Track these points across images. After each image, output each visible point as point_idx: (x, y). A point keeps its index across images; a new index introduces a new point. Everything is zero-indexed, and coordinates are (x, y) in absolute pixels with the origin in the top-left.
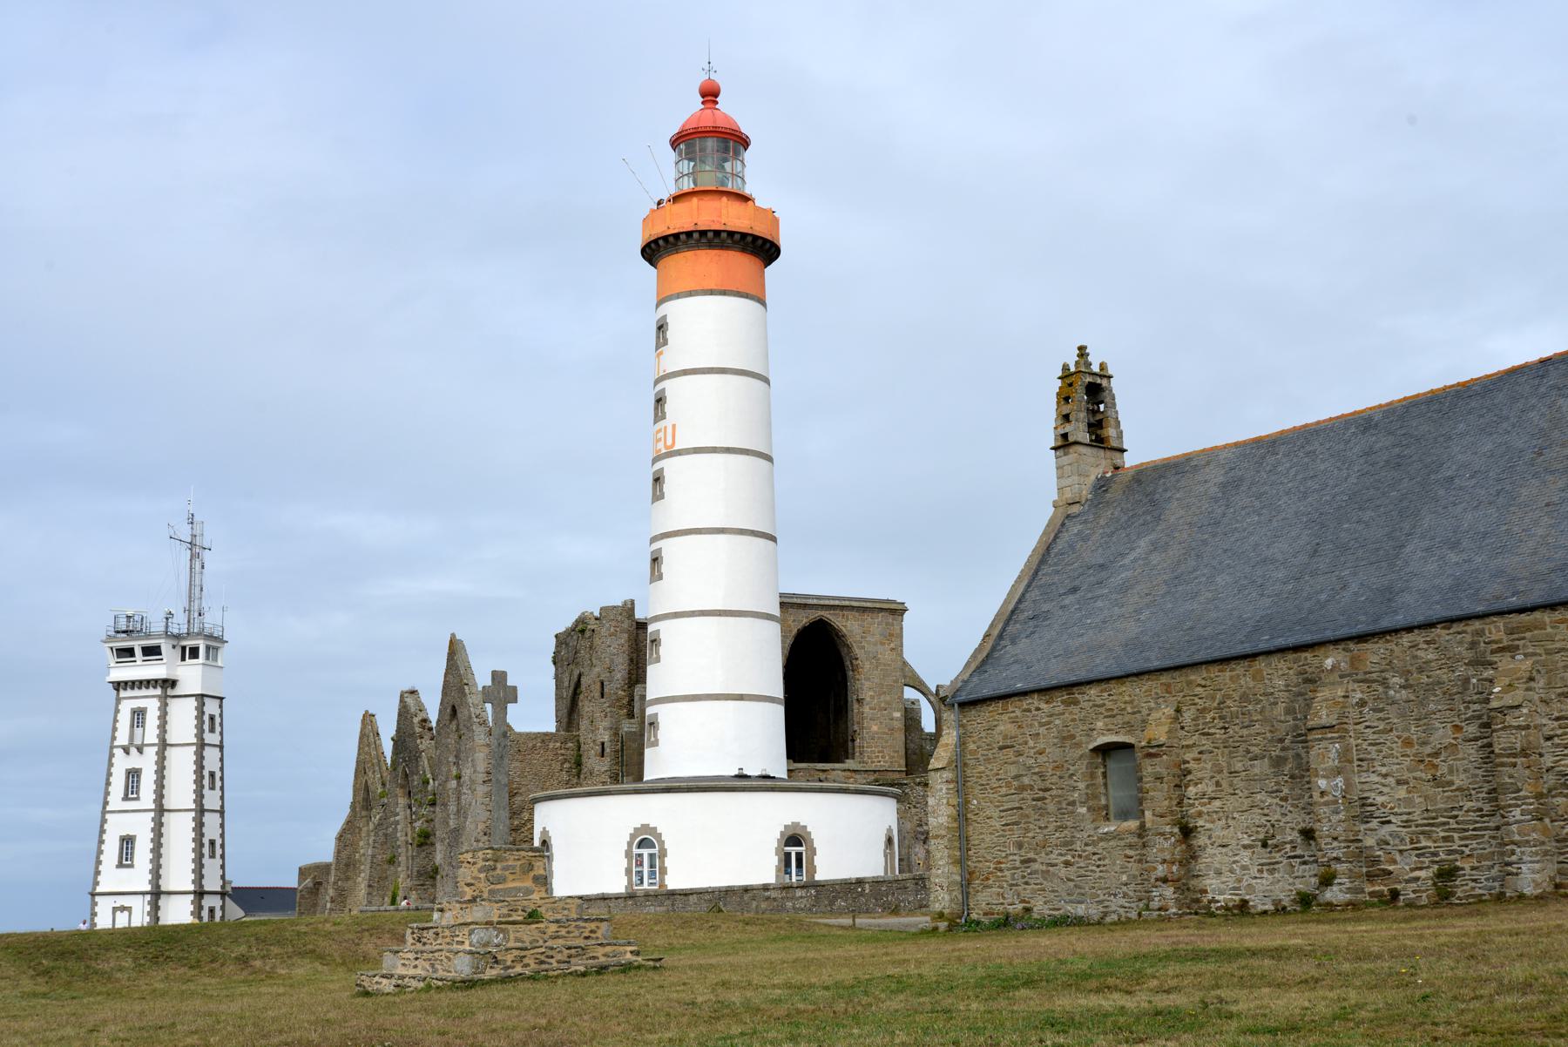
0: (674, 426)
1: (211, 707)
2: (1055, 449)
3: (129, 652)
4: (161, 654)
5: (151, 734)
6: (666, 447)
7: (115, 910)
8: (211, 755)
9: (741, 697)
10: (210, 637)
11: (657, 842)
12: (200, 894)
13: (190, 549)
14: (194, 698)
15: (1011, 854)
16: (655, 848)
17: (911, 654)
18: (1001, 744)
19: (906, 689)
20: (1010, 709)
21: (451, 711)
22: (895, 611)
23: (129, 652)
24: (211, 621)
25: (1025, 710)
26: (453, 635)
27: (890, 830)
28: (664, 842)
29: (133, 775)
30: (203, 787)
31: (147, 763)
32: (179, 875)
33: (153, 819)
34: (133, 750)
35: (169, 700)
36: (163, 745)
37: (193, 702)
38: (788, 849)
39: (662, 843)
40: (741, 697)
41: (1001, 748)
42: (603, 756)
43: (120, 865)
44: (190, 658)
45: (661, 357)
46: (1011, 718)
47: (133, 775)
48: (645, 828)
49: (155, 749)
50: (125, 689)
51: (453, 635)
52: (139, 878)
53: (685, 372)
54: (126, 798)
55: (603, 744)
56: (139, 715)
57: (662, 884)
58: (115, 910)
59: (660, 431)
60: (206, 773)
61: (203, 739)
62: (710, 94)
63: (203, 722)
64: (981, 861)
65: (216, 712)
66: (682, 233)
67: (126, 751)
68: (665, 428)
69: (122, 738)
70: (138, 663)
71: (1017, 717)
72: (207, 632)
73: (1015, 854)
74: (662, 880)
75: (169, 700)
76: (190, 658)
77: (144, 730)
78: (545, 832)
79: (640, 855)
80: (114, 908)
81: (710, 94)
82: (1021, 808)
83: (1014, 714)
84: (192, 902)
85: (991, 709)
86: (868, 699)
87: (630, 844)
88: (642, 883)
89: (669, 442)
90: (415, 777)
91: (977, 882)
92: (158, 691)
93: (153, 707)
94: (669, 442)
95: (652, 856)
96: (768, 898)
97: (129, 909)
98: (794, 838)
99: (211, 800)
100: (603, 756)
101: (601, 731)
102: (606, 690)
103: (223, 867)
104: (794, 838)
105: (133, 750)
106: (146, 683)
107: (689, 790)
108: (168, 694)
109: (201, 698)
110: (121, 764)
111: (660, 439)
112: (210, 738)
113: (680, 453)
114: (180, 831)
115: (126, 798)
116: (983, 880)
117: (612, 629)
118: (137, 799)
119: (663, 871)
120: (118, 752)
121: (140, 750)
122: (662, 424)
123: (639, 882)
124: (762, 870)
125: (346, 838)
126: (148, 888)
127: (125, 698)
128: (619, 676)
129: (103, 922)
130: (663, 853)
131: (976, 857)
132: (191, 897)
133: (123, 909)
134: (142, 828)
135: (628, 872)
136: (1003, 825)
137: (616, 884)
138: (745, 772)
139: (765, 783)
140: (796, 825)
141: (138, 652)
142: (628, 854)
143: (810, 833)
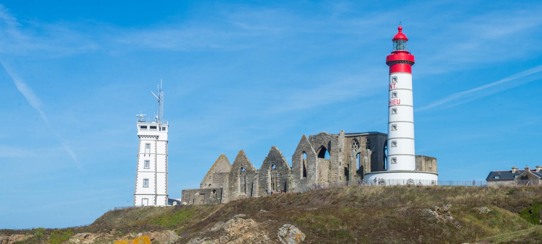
0: (400, 100)
3: (145, 127)
4: (147, 128)
5: (153, 150)
6: (397, 103)
7: (142, 199)
14: (165, 142)
23: (145, 127)
29: (147, 162)
32: (162, 190)
34: (147, 155)
36: (156, 154)
39: (414, 182)
42: (340, 165)
43: (144, 187)
44: (162, 130)
45: (395, 85)
47: (147, 162)
53: (402, 89)
54: (144, 168)
56: (148, 145)
58: (142, 199)
59: (395, 100)
68: (397, 100)
70: (148, 130)
76: (162, 130)
77: (150, 149)
80: (142, 199)
93: (152, 143)
94: (398, 103)
97: (148, 199)
100: (340, 165)
101: (340, 159)
105: (147, 155)
107: (409, 172)
110: (142, 160)
111: (395, 102)
113: (401, 105)
115: (144, 168)
118: (149, 168)
122: (396, 99)
126: (155, 193)
127: (143, 140)
129: (138, 203)
133: (145, 199)
134: (151, 177)
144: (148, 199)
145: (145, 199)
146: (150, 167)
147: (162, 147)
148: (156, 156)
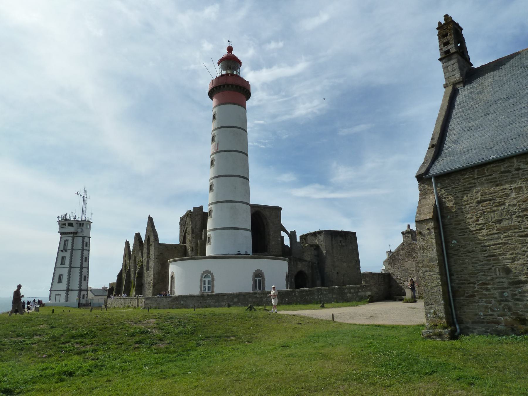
1: (86, 240)
2: (440, 60)
4: (73, 225)
5: (69, 247)
7: (56, 295)
8: (85, 252)
9: (238, 229)
10: (88, 221)
11: (211, 276)
12: (80, 290)
13: (83, 198)
15: (497, 278)
16: (210, 278)
17: (284, 222)
18: (479, 199)
19: (282, 232)
20: (487, 174)
21: (148, 238)
22: (279, 209)
24: (88, 217)
25: (502, 172)
26: (149, 216)
27: (287, 272)
28: (213, 276)
29: (63, 258)
30: (83, 261)
31: (68, 255)
32: (75, 285)
33: (80, 270)
34: (64, 251)
35: (75, 238)
36: (72, 250)
37: (81, 238)
38: (256, 279)
39: (212, 276)
40: (238, 229)
41: (479, 202)
42: (193, 251)
46: (489, 179)
47: (63, 258)
48: (207, 271)
49: (70, 251)
50: (63, 235)
51: (149, 216)
52: (63, 286)
55: (193, 247)
57: (213, 291)
58: (56, 295)
60: (84, 257)
61: (84, 248)
62: (230, 49)
63: (84, 244)
64: (465, 284)
65: (88, 241)
66: (222, 85)
67: (62, 251)
69: (62, 248)
71: (495, 178)
72: (87, 220)
73: (502, 278)
74: (213, 289)
75: (75, 238)
78: (172, 272)
79: (205, 281)
81: (230, 49)
82: (507, 243)
83: (492, 177)
84: (78, 293)
85: (466, 176)
86: (271, 234)
87: (202, 277)
88: (206, 290)
89: (216, 149)
90: (138, 258)
91: (462, 298)
92: (72, 235)
93: (70, 239)
95: (209, 281)
96: (256, 297)
97: (60, 295)
98: (258, 275)
99: (85, 265)
100: (193, 251)
102: (194, 231)
103: (88, 283)
104: (258, 275)
105: (64, 251)
106: (69, 233)
108: (75, 236)
109: (83, 237)
112: (85, 248)
114: (76, 273)
116: (467, 297)
117: (196, 214)
118: (64, 264)
119: (213, 286)
120: (60, 252)
121: (66, 251)
123: (204, 290)
124: (246, 287)
125: (120, 276)
128: (198, 227)
130: (213, 280)
131: (459, 280)
132: (78, 291)
133: (58, 295)
134: (65, 272)
135: (201, 286)
136: (487, 257)
137: (196, 291)
138: (240, 253)
139: (246, 256)
140: (258, 270)
141: (67, 225)
142: (201, 280)
143: (263, 273)
144: (60, 294)
145: (58, 295)
146: (65, 263)
147: (79, 241)
148: (72, 253)
